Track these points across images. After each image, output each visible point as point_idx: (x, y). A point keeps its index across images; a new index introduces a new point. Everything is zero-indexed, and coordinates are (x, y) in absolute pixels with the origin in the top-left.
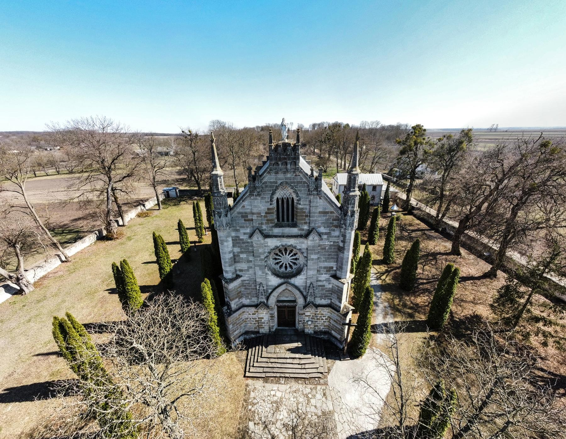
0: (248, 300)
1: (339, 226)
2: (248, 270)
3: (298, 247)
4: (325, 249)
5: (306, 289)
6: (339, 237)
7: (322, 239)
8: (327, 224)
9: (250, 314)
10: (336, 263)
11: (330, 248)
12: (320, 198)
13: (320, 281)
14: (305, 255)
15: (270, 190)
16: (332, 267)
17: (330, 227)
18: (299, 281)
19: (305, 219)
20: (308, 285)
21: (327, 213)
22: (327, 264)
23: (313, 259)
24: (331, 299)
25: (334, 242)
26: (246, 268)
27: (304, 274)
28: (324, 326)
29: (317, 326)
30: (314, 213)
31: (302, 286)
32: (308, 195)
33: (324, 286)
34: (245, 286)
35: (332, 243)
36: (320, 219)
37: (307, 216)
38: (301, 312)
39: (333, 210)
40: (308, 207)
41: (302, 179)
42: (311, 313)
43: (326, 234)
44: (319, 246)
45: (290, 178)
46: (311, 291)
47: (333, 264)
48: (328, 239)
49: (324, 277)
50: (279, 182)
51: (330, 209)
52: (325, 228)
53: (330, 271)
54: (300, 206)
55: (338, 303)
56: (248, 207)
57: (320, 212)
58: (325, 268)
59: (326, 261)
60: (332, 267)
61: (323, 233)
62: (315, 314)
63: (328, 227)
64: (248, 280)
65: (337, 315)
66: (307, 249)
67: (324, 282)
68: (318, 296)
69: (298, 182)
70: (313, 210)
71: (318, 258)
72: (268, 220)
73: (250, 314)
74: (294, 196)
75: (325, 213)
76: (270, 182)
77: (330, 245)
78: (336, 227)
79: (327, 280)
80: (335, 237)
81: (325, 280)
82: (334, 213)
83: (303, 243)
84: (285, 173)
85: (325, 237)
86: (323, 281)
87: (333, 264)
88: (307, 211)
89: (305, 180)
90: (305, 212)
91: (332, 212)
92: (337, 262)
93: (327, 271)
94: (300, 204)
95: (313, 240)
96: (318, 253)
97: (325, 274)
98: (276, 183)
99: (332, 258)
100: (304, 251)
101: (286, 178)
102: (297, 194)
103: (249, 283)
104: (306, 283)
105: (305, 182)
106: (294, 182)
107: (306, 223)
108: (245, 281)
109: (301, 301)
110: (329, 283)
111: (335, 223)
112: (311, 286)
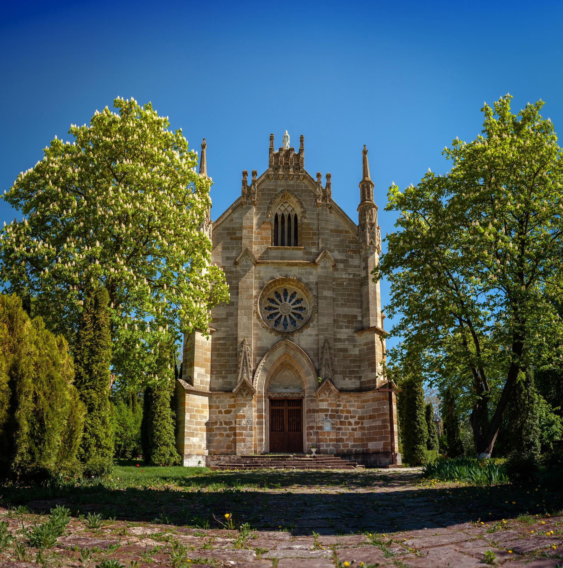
0: (221, 380)
1: (357, 251)
2: (226, 319)
3: (305, 281)
4: (342, 284)
5: (318, 356)
6: (359, 267)
7: (337, 270)
8: (342, 247)
9: (220, 412)
10: (359, 310)
11: (349, 284)
12: (330, 212)
13: (340, 340)
14: (315, 293)
15: (268, 199)
16: (356, 317)
17: (346, 252)
18: (306, 338)
19: (312, 238)
20: (321, 345)
21: (341, 232)
22: (346, 310)
23: (326, 298)
24: (360, 377)
25: (354, 275)
26: (224, 316)
27: (314, 327)
28: (355, 440)
29: (341, 440)
30: (324, 229)
31: (312, 349)
32: (314, 206)
33: (345, 350)
34: (218, 350)
35: (351, 276)
36: (332, 239)
37: (314, 234)
38: (313, 406)
39: (348, 229)
40: (316, 222)
41: (308, 187)
42: (330, 405)
43: (342, 261)
44: (334, 279)
45: (293, 186)
46: (327, 356)
47: (355, 311)
48: (345, 270)
49: (344, 333)
50: (280, 189)
51: (344, 226)
52: (339, 252)
53: (352, 322)
54: (306, 221)
55: (370, 376)
56: (237, 221)
57: (332, 231)
58: (345, 316)
59: (346, 305)
60: (356, 317)
61: (336, 261)
62: (337, 411)
63: (344, 251)
64: (223, 338)
65: (374, 400)
66: (317, 284)
67: (347, 343)
68: (338, 370)
69: (303, 191)
70: (323, 224)
71: (334, 300)
72: (262, 239)
73: (220, 412)
74: (298, 210)
75: (338, 232)
76: (269, 189)
77: (350, 280)
78: (355, 252)
79: (351, 339)
80: (355, 267)
81: (348, 340)
82: (349, 233)
83: (311, 273)
84: (286, 179)
85: (341, 266)
86: (345, 340)
87: (355, 311)
88: (315, 227)
89: (310, 188)
90: (312, 229)
91: (347, 232)
92: (361, 308)
93: (349, 322)
94: (306, 218)
95: (325, 268)
96: (334, 290)
97: (347, 327)
98: (276, 190)
99: (353, 301)
100: (313, 286)
101: (288, 186)
102: (301, 204)
103: (225, 344)
104: (318, 344)
105: (310, 191)
106: (298, 191)
107: (313, 244)
108: (219, 339)
109: (310, 381)
110: (354, 346)
111: (353, 246)
112: (326, 344)
